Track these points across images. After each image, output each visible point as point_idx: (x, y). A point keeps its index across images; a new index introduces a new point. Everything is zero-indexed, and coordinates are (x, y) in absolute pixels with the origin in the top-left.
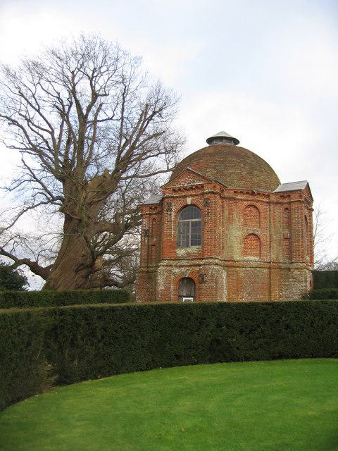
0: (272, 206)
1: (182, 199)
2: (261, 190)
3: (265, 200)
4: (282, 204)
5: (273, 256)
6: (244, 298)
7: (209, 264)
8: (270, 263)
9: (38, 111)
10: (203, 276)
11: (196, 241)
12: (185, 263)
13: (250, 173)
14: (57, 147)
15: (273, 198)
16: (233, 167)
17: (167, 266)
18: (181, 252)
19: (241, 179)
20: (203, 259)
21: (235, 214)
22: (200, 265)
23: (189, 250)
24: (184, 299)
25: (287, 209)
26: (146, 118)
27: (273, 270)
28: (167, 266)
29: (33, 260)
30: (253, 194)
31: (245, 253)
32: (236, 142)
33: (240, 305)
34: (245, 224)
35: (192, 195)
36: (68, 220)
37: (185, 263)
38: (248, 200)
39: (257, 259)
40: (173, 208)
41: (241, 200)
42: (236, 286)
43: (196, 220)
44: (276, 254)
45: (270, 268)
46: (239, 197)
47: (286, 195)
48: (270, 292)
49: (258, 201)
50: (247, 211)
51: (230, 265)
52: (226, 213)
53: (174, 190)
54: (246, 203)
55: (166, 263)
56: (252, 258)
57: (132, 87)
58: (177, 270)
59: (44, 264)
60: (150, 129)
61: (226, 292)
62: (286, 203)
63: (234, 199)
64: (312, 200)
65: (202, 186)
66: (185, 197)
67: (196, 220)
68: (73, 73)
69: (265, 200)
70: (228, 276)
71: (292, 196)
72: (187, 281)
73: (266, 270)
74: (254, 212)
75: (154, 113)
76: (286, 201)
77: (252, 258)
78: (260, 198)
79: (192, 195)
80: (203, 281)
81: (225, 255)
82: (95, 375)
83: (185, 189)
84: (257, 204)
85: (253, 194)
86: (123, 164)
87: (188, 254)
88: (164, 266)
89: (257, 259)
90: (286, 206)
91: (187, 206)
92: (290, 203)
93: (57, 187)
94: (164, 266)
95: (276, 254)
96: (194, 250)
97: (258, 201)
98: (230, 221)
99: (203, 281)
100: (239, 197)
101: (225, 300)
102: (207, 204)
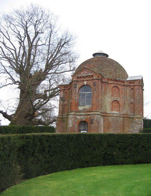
0: (125, 87)
1: (82, 82)
2: (120, 79)
3: (122, 84)
4: (130, 86)
5: (125, 112)
6: (111, 131)
7: (95, 114)
8: (124, 115)
9: (9, 40)
10: (92, 120)
12: (83, 113)
14: (17, 57)
15: (126, 83)
17: (74, 115)
18: (81, 108)
20: (92, 112)
21: (108, 90)
22: (90, 115)
24: (82, 131)
25: (132, 89)
26: (61, 45)
27: (125, 118)
28: (74, 115)
29: (4, 111)
30: (116, 80)
32: (107, 56)
33: (110, 135)
34: (112, 95)
35: (87, 80)
36: (22, 92)
37: (83, 113)
38: (114, 84)
39: (118, 113)
40: (77, 86)
41: (111, 83)
42: (108, 126)
43: (89, 92)
44: (126, 110)
46: (110, 82)
48: (124, 129)
49: (119, 84)
51: (105, 115)
52: (103, 90)
53: (78, 77)
55: (73, 113)
56: (116, 112)
57: (55, 30)
58: (78, 117)
59: (9, 113)
60: (63, 50)
61: (102, 128)
62: (132, 86)
63: (107, 83)
64: (143, 85)
65: (92, 76)
66: (84, 81)
67: (89, 92)
68: (26, 22)
69: (122, 84)
70: (104, 121)
71: (135, 82)
72: (83, 123)
73: (122, 118)
74: (117, 90)
75: (65, 43)
76: (132, 85)
77: (116, 112)
78: (120, 83)
79: (87, 80)
80: (92, 123)
81: (102, 111)
82: (44, 173)
83: (84, 77)
84: (118, 86)
85: (116, 80)
86: (49, 66)
87: (84, 109)
88: (72, 115)
89: (118, 113)
90: (132, 87)
91: (84, 85)
92: (134, 86)
93: (17, 78)
94: (72, 115)
95: (126, 110)
97: (119, 84)
98: (105, 94)
99: (92, 123)
100: (110, 82)
101: (102, 132)
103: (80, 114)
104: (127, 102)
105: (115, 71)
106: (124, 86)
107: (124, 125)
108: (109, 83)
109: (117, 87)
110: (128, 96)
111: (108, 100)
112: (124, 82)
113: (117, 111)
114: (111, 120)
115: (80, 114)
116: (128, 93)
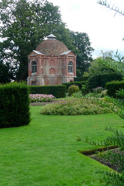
2: (55, 55)
3: (56, 58)
4: (62, 59)
5: (59, 74)
6: (50, 85)
7: (38, 77)
11: (36, 72)
13: (52, 50)
16: (48, 48)
18: (32, 74)
19: (49, 52)
21: (47, 63)
22: (36, 78)
23: (34, 74)
31: (50, 74)
33: (50, 87)
37: (33, 77)
42: (47, 82)
44: (59, 73)
45: (57, 78)
46: (48, 58)
47: (62, 56)
49: (54, 58)
50: (51, 61)
52: (44, 63)
53: (30, 57)
54: (50, 59)
56: (53, 75)
58: (31, 79)
63: (47, 58)
65: (36, 56)
66: (33, 59)
72: (33, 83)
73: (56, 78)
74: (53, 62)
76: (63, 57)
77: (53, 75)
78: (55, 58)
83: (33, 56)
89: (54, 75)
90: (63, 59)
92: (63, 58)
95: (59, 73)
96: (35, 73)
97: (54, 58)
98: (45, 65)
99: (36, 82)
100: (48, 58)
102: (37, 61)
103: (32, 77)
104: (60, 69)
105: (52, 50)
106: (58, 59)
107: (57, 82)
108: (48, 59)
109: (53, 60)
110: (61, 64)
111: (48, 68)
112: (58, 56)
113: (54, 74)
114: (49, 80)
115: (32, 77)
116: (61, 63)
